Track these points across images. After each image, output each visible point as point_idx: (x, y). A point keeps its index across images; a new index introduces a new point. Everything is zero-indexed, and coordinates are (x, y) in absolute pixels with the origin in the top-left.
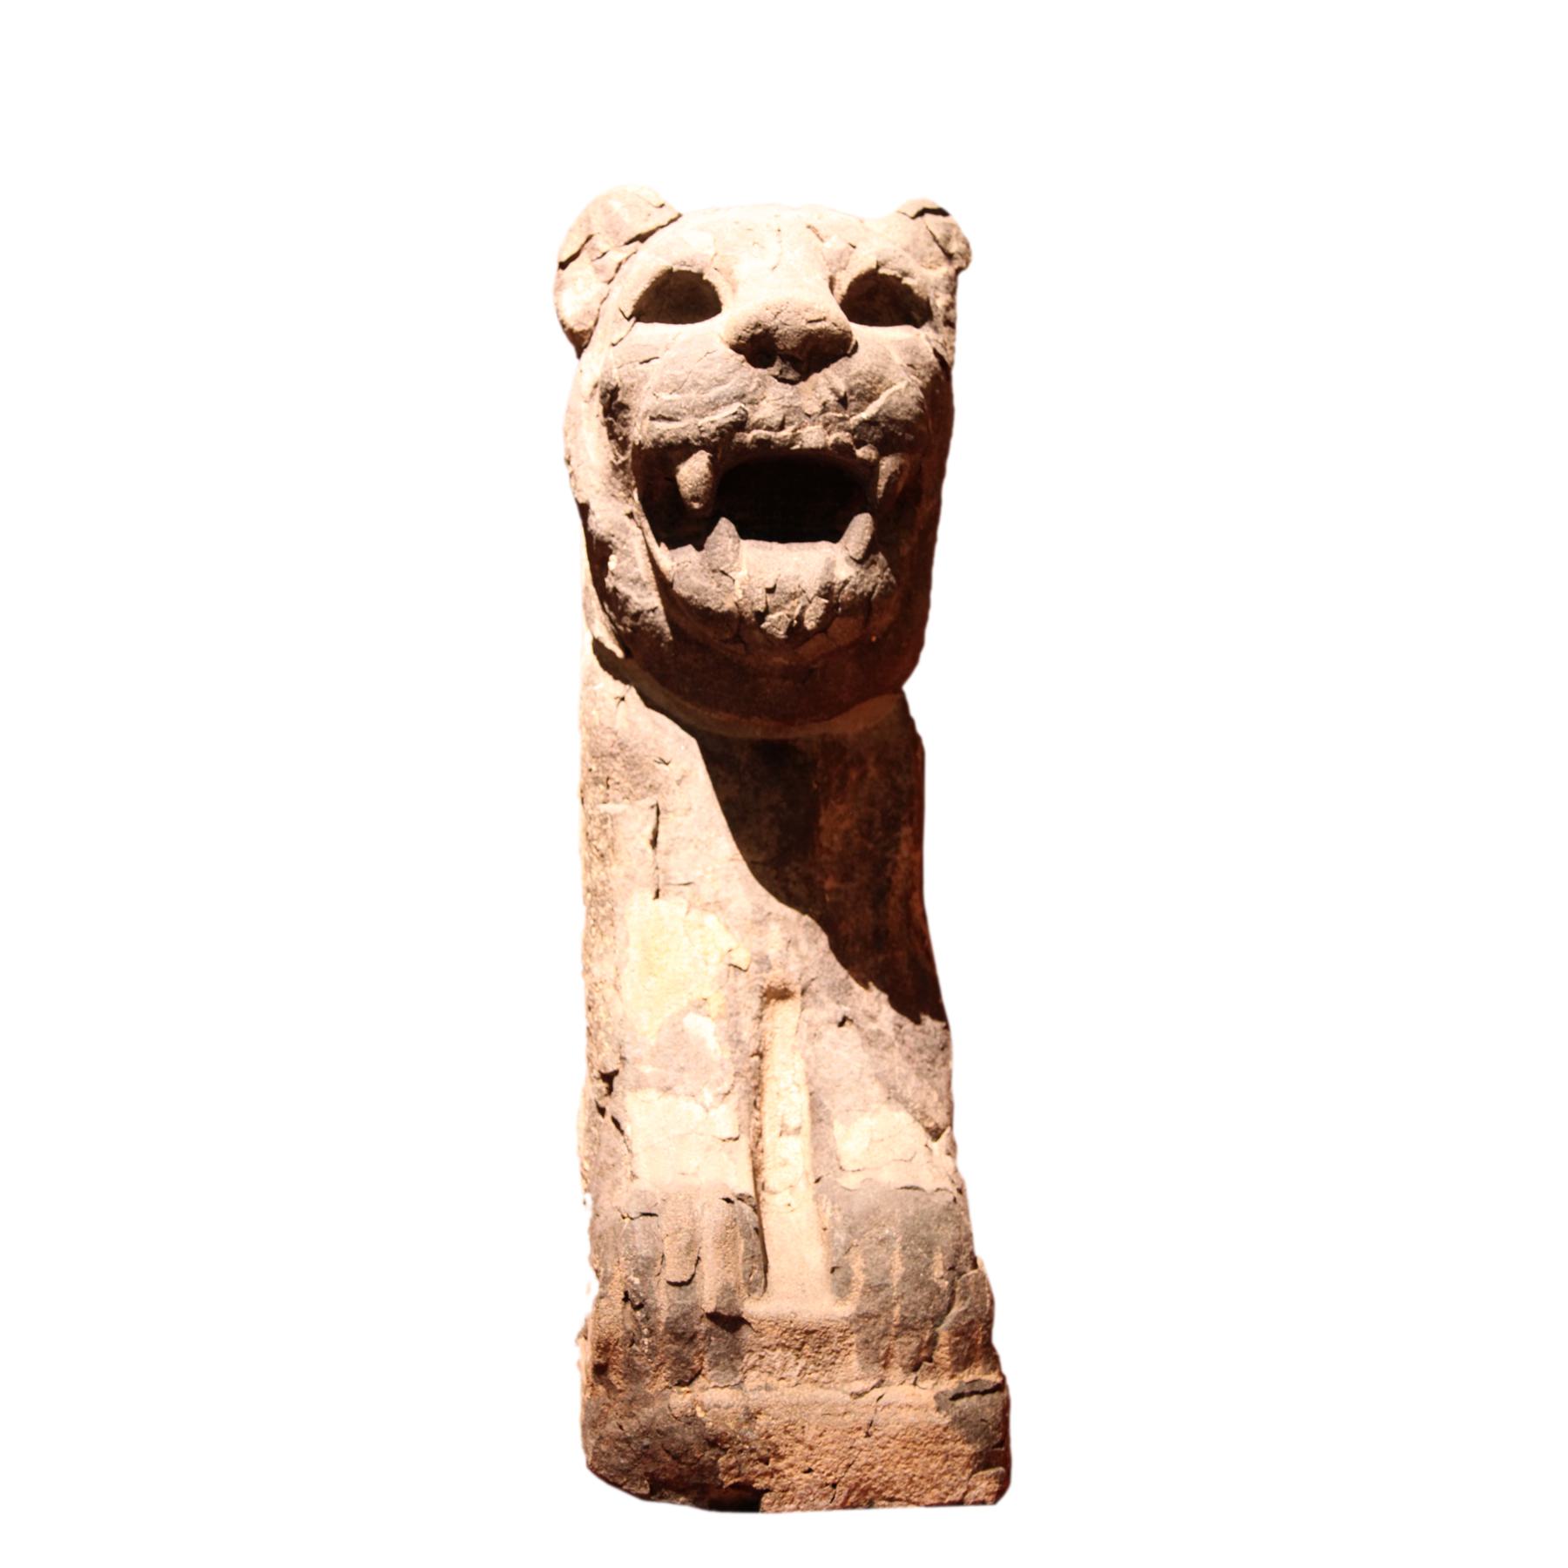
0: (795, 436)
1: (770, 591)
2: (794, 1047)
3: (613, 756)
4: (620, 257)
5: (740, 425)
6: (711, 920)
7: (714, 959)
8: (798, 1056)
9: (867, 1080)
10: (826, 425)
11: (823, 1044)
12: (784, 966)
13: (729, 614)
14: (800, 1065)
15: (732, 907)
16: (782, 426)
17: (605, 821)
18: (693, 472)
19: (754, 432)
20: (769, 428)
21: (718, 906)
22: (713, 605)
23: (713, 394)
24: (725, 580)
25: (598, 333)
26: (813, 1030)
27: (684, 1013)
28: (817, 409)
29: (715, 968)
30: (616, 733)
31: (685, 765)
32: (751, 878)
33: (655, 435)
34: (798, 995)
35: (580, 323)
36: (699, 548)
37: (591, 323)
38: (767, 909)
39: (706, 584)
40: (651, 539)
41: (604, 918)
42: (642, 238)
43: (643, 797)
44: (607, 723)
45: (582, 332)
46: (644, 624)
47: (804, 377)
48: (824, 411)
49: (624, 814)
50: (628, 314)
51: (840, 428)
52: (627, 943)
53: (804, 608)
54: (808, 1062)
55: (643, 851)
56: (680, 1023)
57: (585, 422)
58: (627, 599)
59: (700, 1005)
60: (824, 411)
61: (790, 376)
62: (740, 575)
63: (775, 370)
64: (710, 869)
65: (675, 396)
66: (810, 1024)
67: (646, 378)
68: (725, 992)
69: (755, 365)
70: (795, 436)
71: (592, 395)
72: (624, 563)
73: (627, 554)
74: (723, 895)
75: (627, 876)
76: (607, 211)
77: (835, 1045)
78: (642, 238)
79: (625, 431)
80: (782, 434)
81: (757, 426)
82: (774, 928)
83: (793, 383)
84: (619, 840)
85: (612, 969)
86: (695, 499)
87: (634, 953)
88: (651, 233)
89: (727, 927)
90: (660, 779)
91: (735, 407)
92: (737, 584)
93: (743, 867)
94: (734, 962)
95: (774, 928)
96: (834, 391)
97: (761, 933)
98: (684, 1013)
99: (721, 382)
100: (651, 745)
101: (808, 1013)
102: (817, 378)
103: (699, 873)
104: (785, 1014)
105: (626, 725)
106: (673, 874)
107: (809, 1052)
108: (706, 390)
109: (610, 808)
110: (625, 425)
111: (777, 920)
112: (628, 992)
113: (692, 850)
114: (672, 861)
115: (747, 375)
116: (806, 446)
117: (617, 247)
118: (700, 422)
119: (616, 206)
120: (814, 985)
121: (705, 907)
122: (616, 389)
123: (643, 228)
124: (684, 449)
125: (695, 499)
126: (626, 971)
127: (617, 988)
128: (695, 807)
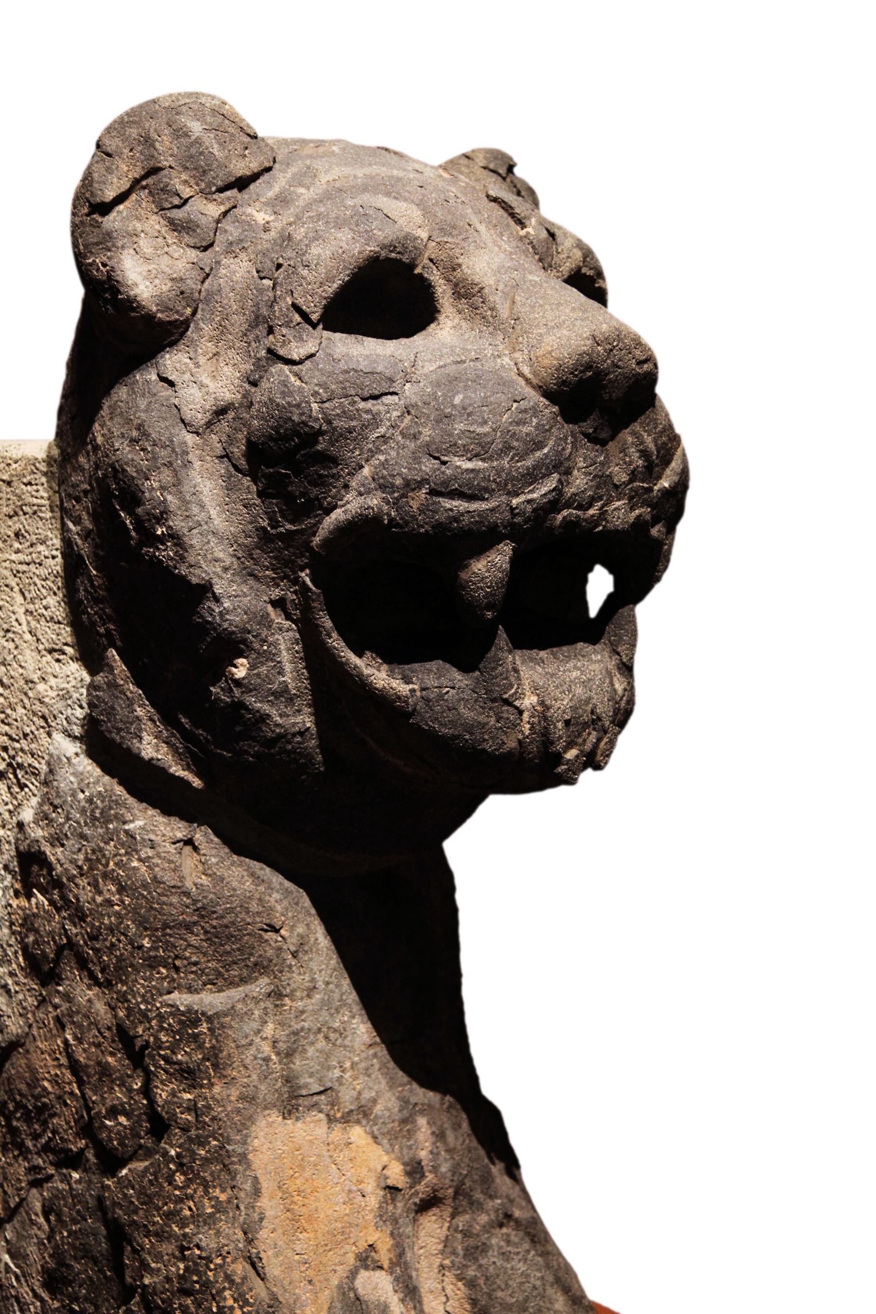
0: (603, 513)
1: (567, 723)
2: (442, 1267)
3: (188, 927)
4: (214, 210)
5: (555, 503)
6: (357, 1134)
7: (370, 1186)
8: (450, 1277)
9: (550, 1291)
10: (631, 499)
11: (492, 1258)
12: (435, 1169)
13: (510, 753)
14: (457, 1291)
15: (378, 1109)
16: (590, 505)
17: (195, 1023)
18: (490, 567)
19: (565, 513)
20: (580, 507)
21: (362, 1113)
22: (489, 747)
23: (529, 462)
24: (508, 713)
25: (203, 331)
26: (471, 1242)
27: (353, 1274)
28: (625, 478)
29: (373, 1201)
30: (187, 894)
31: (301, 929)
32: (392, 1065)
33: (441, 517)
34: (449, 1201)
35: (168, 309)
36: (465, 668)
37: (189, 311)
38: (413, 1100)
39: (482, 718)
40: (336, 642)
41: (206, 1161)
42: (242, 183)
43: (243, 981)
44: (169, 878)
45: (173, 323)
46: (283, 751)
47: (613, 438)
48: (631, 481)
49: (231, 1011)
50: (315, 317)
51: (645, 503)
52: (257, 1192)
53: (599, 740)
54: (471, 1284)
55: (267, 1060)
56: (353, 1289)
57: (197, 464)
58: (264, 718)
59: (366, 1260)
60: (631, 481)
61: (604, 435)
62: (529, 701)
63: (588, 426)
64: (348, 1064)
65: (479, 464)
66: (467, 1234)
67: (375, 421)
68: (389, 1229)
69: (567, 422)
70: (603, 513)
71: (209, 424)
72: (263, 669)
73: (270, 656)
74: (367, 1095)
75: (242, 1098)
76: (180, 133)
77: (506, 1256)
78: (242, 183)
79: (314, 492)
80: (591, 512)
81: (568, 505)
82: (422, 1121)
83: (603, 443)
84: (229, 1048)
85: (240, 1235)
86: (490, 607)
87: (269, 1204)
88: (255, 177)
89: (375, 1138)
90: (270, 953)
91: (551, 483)
92: (526, 716)
93: (382, 1051)
94: (390, 1182)
95: (422, 1121)
96: (644, 454)
97: (410, 1134)
98: (353, 1274)
99: (539, 446)
100: (254, 907)
101: (461, 1221)
102: (627, 436)
103: (337, 1073)
104: (432, 1229)
105: (204, 880)
106: (305, 1080)
107: (471, 1272)
108: (522, 458)
109: (181, 999)
110: (321, 482)
111: (422, 1112)
112: (273, 1268)
113: (321, 1044)
114: (298, 1063)
115: (560, 437)
116: (610, 526)
117: (206, 194)
118: (515, 502)
119: (196, 128)
120: (468, 1184)
121: (347, 1119)
122: (320, 432)
123: (241, 168)
124: (482, 538)
125: (490, 607)
126: (263, 1234)
127: (254, 1263)
128: (321, 985)
